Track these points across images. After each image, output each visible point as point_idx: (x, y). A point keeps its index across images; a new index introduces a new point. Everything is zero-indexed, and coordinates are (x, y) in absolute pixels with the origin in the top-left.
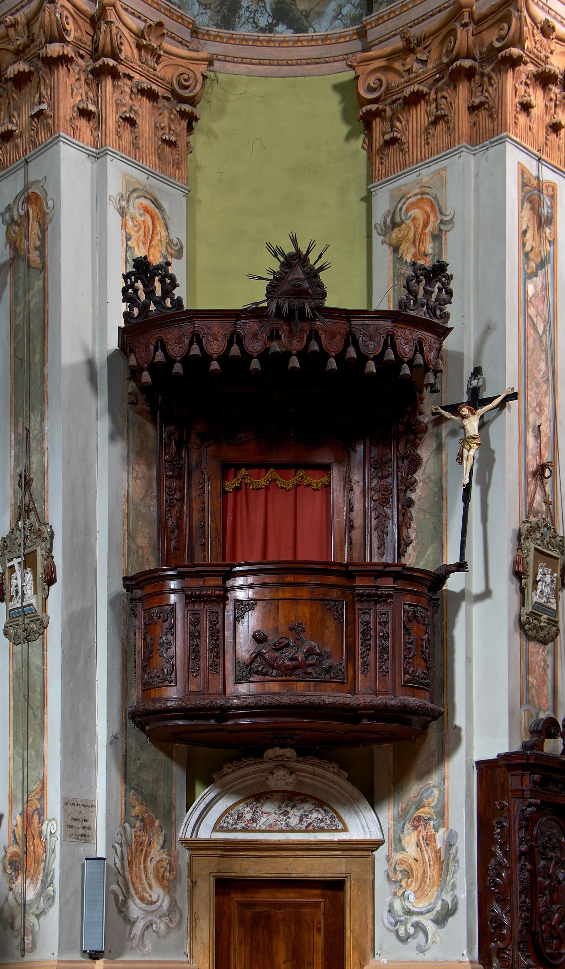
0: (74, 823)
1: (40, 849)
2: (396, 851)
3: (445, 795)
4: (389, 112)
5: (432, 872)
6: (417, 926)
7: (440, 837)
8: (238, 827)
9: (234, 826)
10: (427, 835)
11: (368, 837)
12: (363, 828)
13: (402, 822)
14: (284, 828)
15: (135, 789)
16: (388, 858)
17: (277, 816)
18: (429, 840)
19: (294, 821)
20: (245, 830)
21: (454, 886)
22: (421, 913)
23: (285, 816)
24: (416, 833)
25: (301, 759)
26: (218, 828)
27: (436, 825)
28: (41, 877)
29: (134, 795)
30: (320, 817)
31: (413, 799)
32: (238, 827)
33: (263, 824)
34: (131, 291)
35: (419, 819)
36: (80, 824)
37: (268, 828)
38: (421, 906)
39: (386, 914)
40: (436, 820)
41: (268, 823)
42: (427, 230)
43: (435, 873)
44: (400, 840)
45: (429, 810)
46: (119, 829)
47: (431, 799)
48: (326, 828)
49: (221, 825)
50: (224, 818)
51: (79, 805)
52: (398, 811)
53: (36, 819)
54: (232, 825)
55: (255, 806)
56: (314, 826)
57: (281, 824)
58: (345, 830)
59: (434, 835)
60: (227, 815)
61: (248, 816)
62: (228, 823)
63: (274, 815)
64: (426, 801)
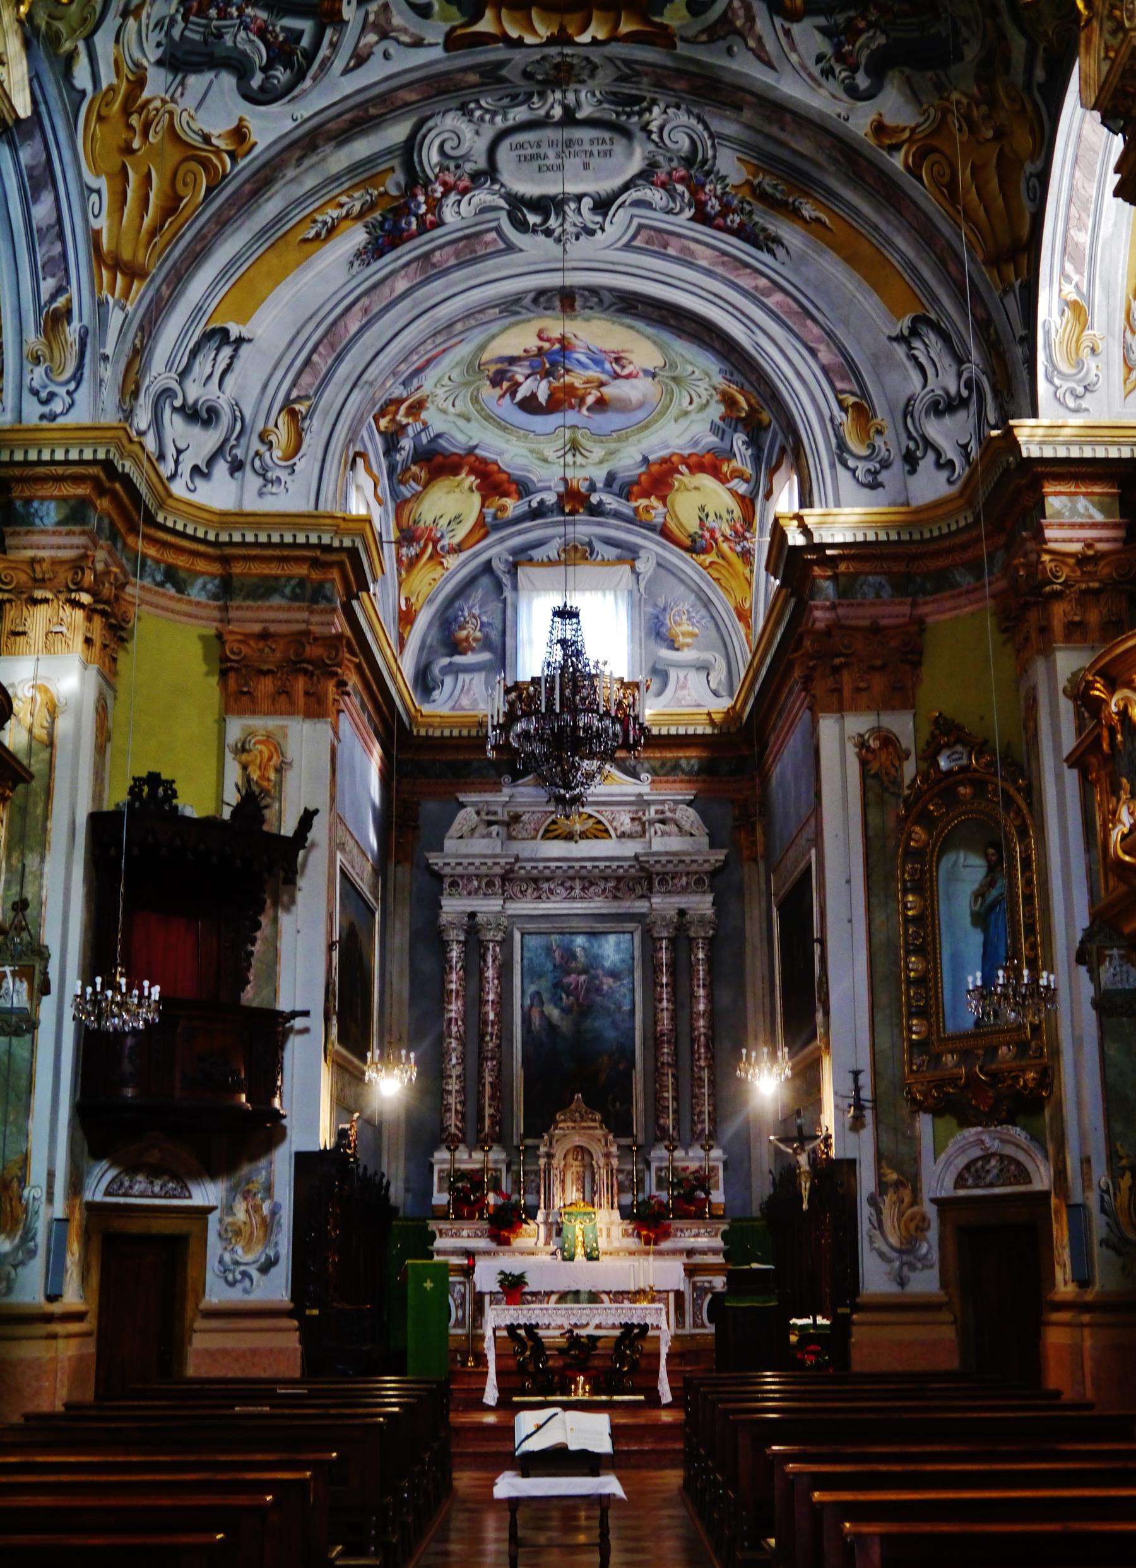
1: (19, 1210)
2: (228, 1214)
5: (258, 1233)
6: (245, 1274)
7: (266, 1209)
11: (206, 1204)
16: (221, 1221)
18: (257, 1209)
19: (157, 1189)
20: (125, 1195)
21: (276, 1244)
22: (247, 1264)
28: (19, 1233)
32: (122, 1191)
35: (249, 1191)
38: (249, 1258)
39: (216, 1264)
42: (272, 763)
43: (261, 1234)
44: (231, 1208)
53: (15, 1184)
58: (190, 1197)
61: (127, 1184)
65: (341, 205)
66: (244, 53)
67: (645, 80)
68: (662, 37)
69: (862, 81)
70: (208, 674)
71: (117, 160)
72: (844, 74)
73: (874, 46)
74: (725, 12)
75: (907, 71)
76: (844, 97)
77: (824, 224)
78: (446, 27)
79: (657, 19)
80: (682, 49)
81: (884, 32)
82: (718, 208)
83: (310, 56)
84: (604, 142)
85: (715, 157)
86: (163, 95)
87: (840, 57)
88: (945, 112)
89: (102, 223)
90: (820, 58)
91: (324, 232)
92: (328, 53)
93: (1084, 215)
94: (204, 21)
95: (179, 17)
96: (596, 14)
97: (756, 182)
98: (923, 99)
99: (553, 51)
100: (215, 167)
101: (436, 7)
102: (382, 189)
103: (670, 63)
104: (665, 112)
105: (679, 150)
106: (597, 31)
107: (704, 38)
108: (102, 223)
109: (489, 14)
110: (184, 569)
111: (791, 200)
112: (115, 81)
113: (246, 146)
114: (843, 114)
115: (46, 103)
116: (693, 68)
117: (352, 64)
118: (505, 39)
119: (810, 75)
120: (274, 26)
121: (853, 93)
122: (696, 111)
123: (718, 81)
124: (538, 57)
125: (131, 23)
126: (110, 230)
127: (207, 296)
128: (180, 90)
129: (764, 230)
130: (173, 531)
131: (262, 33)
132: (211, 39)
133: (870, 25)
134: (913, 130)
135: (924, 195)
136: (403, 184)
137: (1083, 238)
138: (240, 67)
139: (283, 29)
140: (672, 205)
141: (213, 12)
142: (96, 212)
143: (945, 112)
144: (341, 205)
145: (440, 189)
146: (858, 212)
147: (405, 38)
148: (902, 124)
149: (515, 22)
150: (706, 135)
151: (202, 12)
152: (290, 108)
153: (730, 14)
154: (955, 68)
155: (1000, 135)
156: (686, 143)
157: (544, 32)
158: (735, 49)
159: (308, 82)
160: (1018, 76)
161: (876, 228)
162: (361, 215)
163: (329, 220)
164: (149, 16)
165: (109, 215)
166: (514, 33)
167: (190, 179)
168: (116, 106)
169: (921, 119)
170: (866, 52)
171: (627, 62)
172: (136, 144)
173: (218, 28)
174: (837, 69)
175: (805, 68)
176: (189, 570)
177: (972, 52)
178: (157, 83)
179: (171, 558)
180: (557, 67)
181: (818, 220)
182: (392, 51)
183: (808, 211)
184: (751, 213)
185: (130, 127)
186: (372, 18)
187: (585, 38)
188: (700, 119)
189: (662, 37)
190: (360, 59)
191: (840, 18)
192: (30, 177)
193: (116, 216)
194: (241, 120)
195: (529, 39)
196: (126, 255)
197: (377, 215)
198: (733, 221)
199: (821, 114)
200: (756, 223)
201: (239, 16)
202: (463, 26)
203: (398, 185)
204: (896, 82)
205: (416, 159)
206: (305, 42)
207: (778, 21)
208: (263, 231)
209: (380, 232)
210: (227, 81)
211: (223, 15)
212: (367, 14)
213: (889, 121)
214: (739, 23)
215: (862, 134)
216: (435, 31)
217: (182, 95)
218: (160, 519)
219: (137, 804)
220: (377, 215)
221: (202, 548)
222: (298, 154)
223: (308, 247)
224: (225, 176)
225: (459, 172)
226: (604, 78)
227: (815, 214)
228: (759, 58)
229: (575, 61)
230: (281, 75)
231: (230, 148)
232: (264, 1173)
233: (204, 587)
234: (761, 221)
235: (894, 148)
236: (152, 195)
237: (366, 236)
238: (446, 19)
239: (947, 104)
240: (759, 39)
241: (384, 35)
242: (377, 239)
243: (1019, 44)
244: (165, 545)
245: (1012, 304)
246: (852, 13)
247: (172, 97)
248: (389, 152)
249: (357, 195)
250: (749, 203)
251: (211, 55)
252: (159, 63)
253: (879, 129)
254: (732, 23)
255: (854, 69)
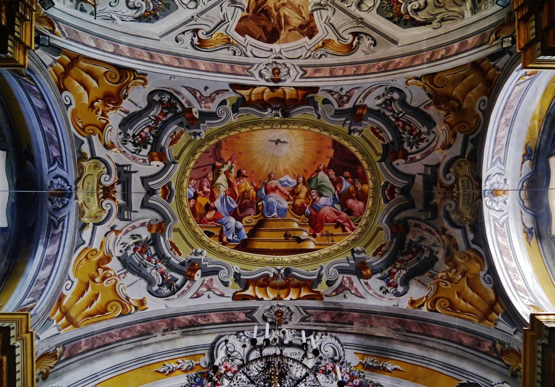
65: (179, 363)
66: (153, 278)
67: (312, 319)
68: (318, 296)
69: (400, 289)
71: (87, 279)
72: (392, 290)
73: (401, 276)
74: (341, 283)
75: (417, 278)
76: (395, 298)
77: (399, 370)
78: (234, 291)
79: (315, 290)
80: (326, 299)
81: (404, 269)
82: (349, 378)
83: (179, 288)
84: (296, 354)
85: (344, 355)
86: (116, 272)
87: (389, 285)
88: (437, 284)
89: (69, 294)
90: (381, 289)
91: (167, 372)
92: (186, 289)
93: (516, 274)
94: (141, 257)
95: (132, 248)
96: (291, 289)
97: (364, 362)
98: (427, 284)
99: (275, 303)
100: (127, 309)
101: (231, 283)
102: (198, 362)
103: (322, 306)
104: (321, 338)
105: (328, 355)
106: (293, 295)
107: (334, 294)
108: (69, 294)
109: (251, 288)
111: (381, 365)
112: (99, 249)
113: (143, 307)
114: (396, 304)
115: (67, 227)
116: (331, 306)
117: (195, 296)
118: (257, 298)
119: (379, 296)
120: (167, 273)
121: (398, 295)
122: (334, 334)
123: (342, 310)
124: (269, 307)
125: (113, 233)
126: (70, 299)
127: (104, 372)
128: (123, 275)
129: (371, 382)
131: (162, 274)
132: (142, 265)
133: (398, 269)
134: (427, 297)
135: (442, 317)
136: (208, 363)
137: (520, 283)
138: (150, 282)
139: (170, 275)
140: (328, 381)
141: (146, 256)
142: (68, 288)
143: (437, 284)
144: (179, 363)
145: (224, 369)
146: (412, 355)
147: (218, 293)
148: (421, 297)
149: (260, 291)
150: (339, 345)
151: (140, 252)
152: (166, 302)
153: (343, 283)
154: (437, 265)
155: (464, 274)
156: (331, 352)
157: (272, 296)
158: (347, 295)
159: (175, 296)
160: (462, 246)
161: (423, 358)
162: (186, 371)
163: (171, 367)
164: (121, 238)
165: (73, 294)
166: (260, 297)
167: (115, 307)
168: (96, 259)
169: (430, 290)
170: (399, 279)
171: (305, 309)
172: (97, 280)
173: (146, 263)
174: (389, 289)
175: (376, 294)
177: (441, 255)
178: (115, 265)
180: (276, 313)
181: (395, 369)
182: (211, 296)
183: (390, 366)
184: (364, 376)
185: (98, 272)
186: (205, 282)
187: (288, 298)
188: (336, 338)
189: (318, 296)
190: (198, 295)
191: (386, 272)
192: (46, 260)
193: (76, 298)
194: (144, 298)
195: (265, 299)
196: (73, 314)
197: (193, 373)
198: (356, 383)
199: (386, 307)
200: (367, 380)
201: (155, 264)
202: (240, 291)
203: (205, 362)
204: (414, 284)
205: (215, 353)
206: (178, 283)
207: (362, 281)
208: (139, 359)
209: (193, 382)
210: (143, 283)
211: (149, 259)
212: (204, 280)
213: (415, 298)
214: (347, 286)
215: (406, 308)
216: (229, 292)
217: (123, 278)
220: (193, 373)
222: (164, 327)
223: (159, 375)
224: (130, 314)
225: (233, 363)
226: (295, 321)
227: (393, 367)
228: (357, 296)
229: (284, 310)
230: (166, 290)
231: (136, 305)
234: (369, 379)
235: (420, 307)
236: (95, 303)
237: (187, 381)
238: (234, 288)
239: (438, 280)
240: (356, 289)
241: (209, 289)
242: (192, 384)
243: (457, 234)
245: (502, 326)
246: (390, 268)
247: (119, 275)
248: (204, 346)
249: (186, 361)
250: (362, 372)
251: (140, 271)
252: (119, 258)
253: (412, 303)
254: (344, 286)
255: (396, 286)
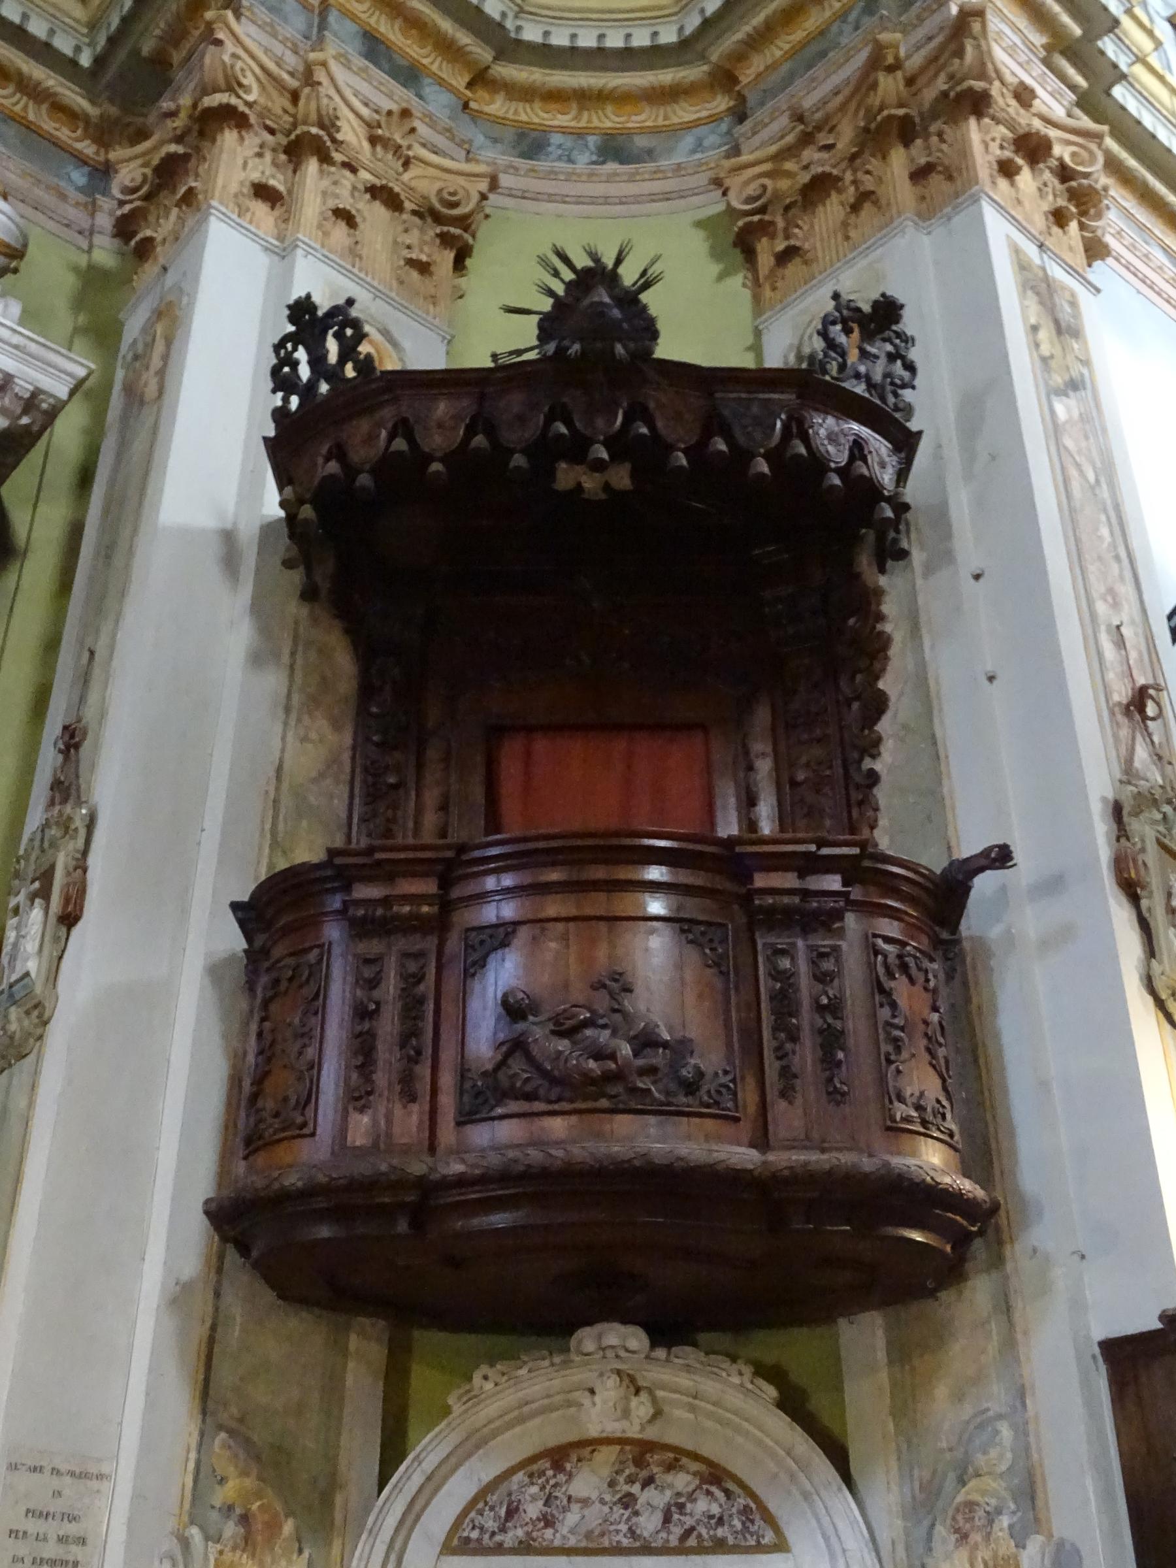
0: (33, 1526)
3: (1032, 1439)
4: (780, 223)
8: (509, 1539)
9: (498, 1538)
10: (995, 1557)
12: (824, 1535)
13: (926, 1523)
14: (625, 1542)
15: (231, 1432)
17: (606, 1509)
19: (649, 1524)
23: (626, 1508)
24: (963, 1554)
25: (661, 1353)
26: (455, 1542)
27: (1017, 1527)
29: (225, 1446)
30: (715, 1509)
31: (948, 1456)
32: (509, 1539)
33: (572, 1531)
34: (286, 369)
35: (971, 1505)
36: (52, 1528)
37: (583, 1544)
40: (1014, 1513)
41: (583, 1530)
45: (994, 1485)
46: (172, 1545)
47: (993, 1453)
48: (731, 1541)
49: (465, 1534)
50: (473, 1514)
51: (56, 1471)
52: (912, 1490)
54: (493, 1534)
55: (552, 1482)
56: (700, 1536)
57: (618, 1531)
59: (1016, 1557)
60: (480, 1505)
61: (533, 1510)
62: (482, 1528)
63: (597, 1505)
64: (980, 1460)
70: (721, 277)
110: (642, 131)
130: (572, 57)
176: (655, 131)
179: (608, 119)
218: (532, 34)
219: (294, 401)
221: (666, 77)
232: (1006, 1432)
233: (699, 146)
244: (585, 98)
